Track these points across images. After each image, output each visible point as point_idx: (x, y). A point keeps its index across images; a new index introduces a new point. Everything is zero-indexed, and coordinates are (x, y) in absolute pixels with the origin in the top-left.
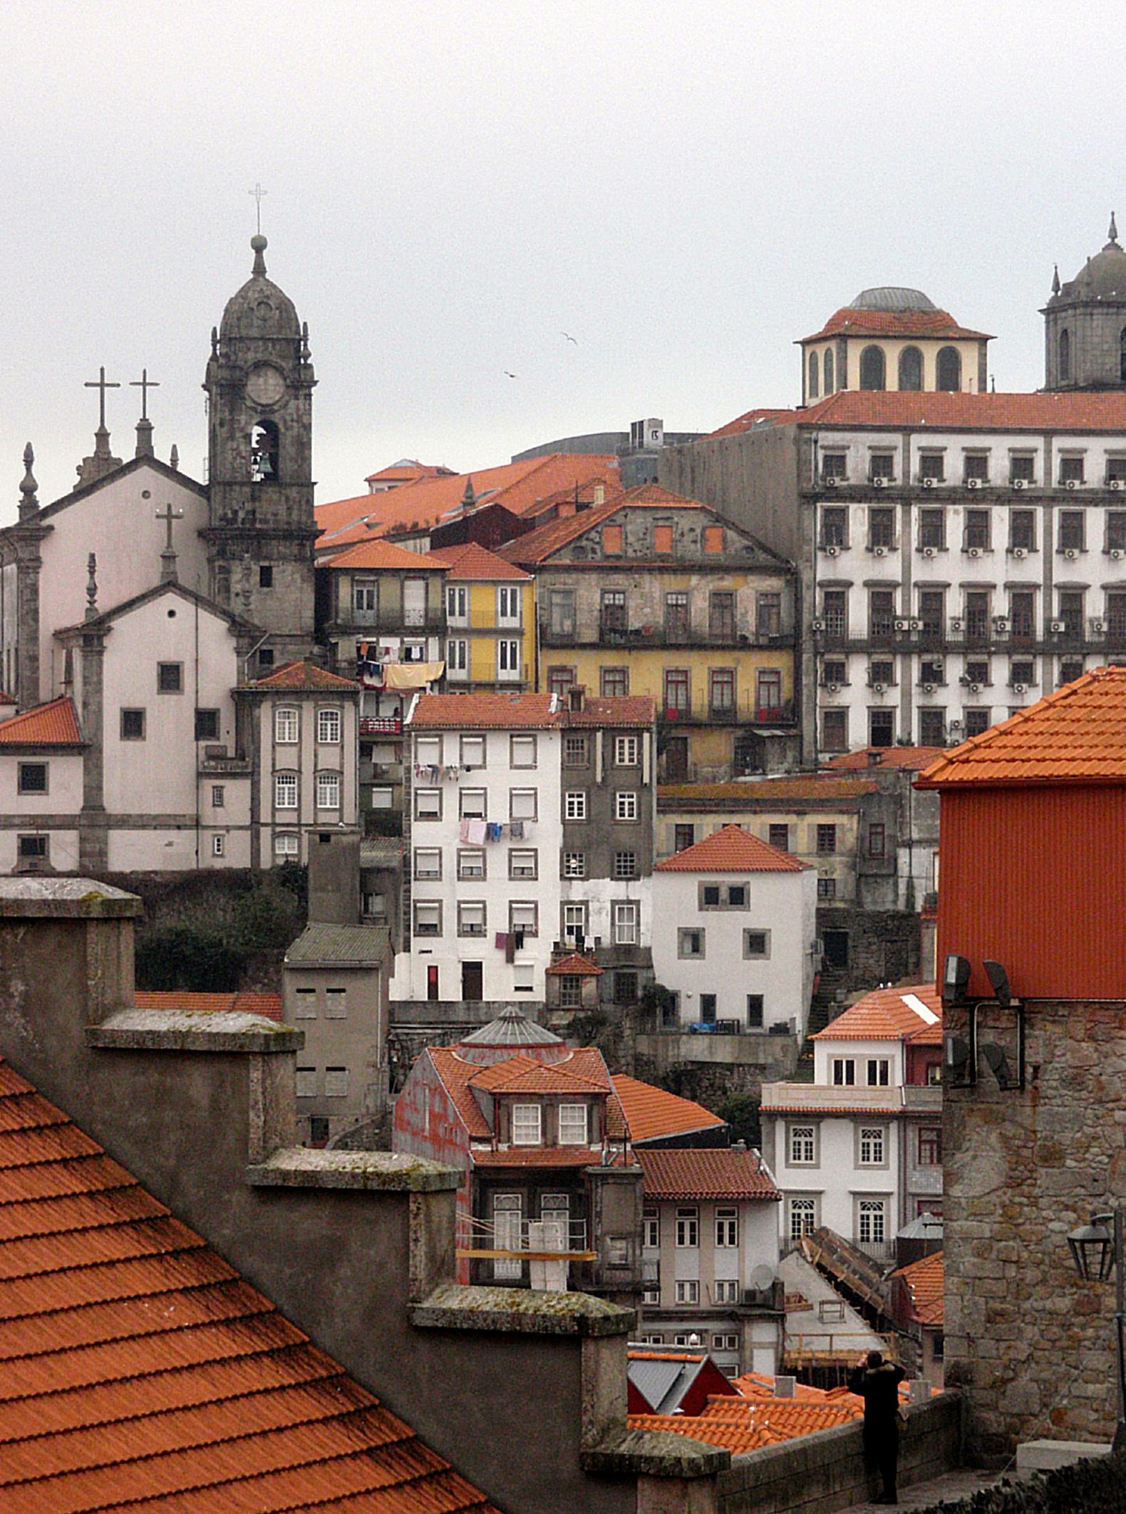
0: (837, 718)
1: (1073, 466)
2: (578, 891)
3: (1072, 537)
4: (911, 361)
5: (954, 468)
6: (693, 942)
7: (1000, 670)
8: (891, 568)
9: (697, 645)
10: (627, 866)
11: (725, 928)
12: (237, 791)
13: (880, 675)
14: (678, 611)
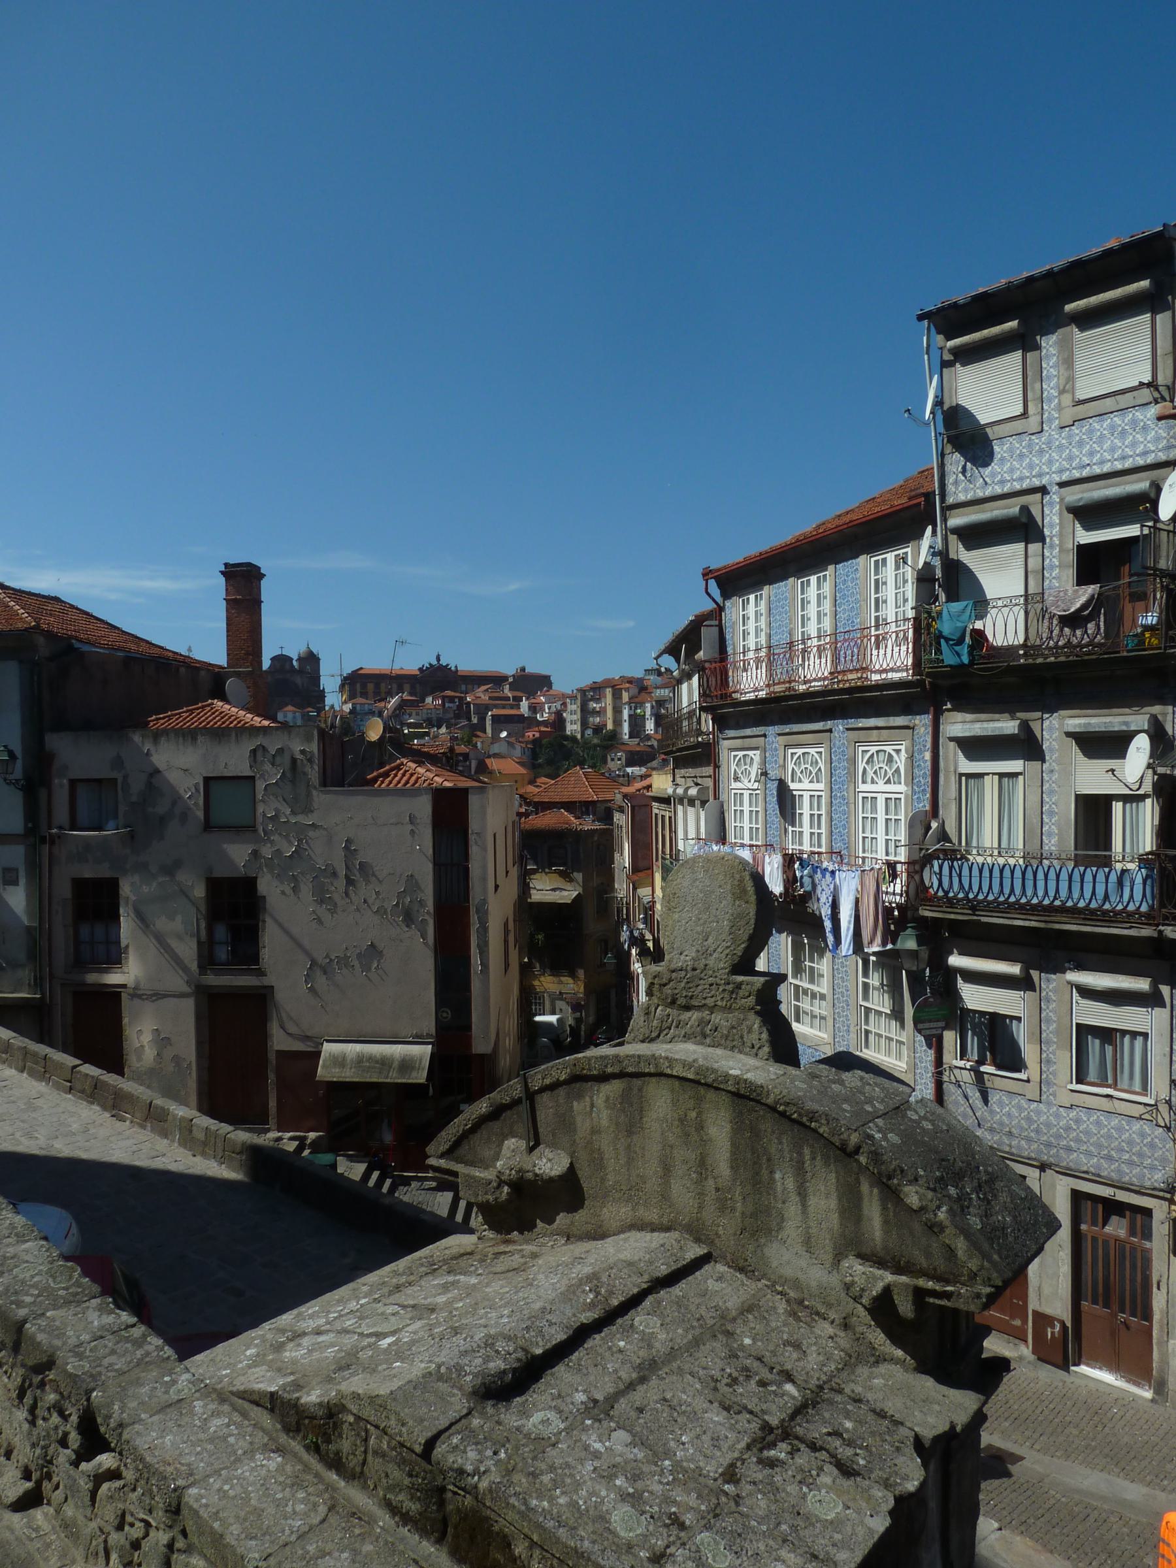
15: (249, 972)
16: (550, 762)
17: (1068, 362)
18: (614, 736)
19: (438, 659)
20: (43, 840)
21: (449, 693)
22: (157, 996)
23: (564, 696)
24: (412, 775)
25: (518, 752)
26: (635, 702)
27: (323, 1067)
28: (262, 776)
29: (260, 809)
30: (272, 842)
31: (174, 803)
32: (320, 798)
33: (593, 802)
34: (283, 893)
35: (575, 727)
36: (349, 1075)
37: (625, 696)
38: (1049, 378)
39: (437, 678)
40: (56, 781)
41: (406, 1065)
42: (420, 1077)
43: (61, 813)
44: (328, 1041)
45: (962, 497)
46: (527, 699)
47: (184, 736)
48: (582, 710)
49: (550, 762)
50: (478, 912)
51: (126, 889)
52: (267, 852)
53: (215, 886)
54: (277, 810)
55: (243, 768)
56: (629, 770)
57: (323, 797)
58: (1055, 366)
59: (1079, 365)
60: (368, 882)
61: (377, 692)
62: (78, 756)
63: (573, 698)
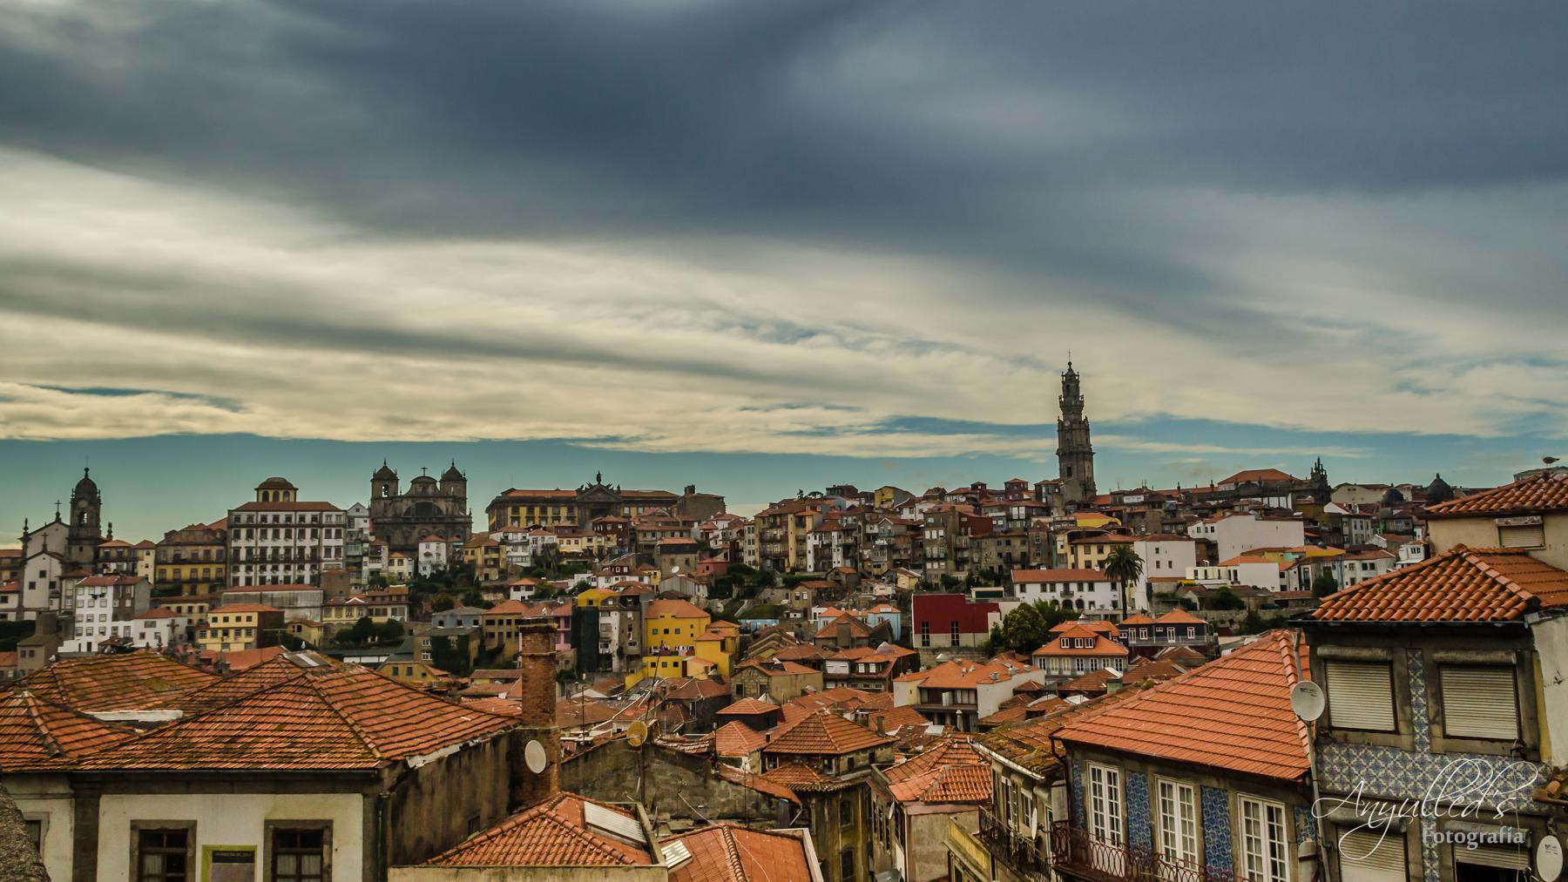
0: (236, 580)
1: (302, 518)
2: (116, 624)
3: (302, 535)
4: (276, 496)
5: (270, 520)
6: (143, 636)
7: (281, 567)
8: (252, 543)
9: (200, 563)
10: (128, 618)
11: (150, 632)
12: (56, 601)
13: (249, 569)
14: (195, 555)
17: (1439, 699)
19: (599, 478)
21: (611, 518)
33: (838, 756)
35: (752, 558)
38: (1419, 706)
39: (598, 504)
45: (1338, 787)
56: (815, 610)
58: (1424, 696)
59: (1448, 705)
61: (529, 518)
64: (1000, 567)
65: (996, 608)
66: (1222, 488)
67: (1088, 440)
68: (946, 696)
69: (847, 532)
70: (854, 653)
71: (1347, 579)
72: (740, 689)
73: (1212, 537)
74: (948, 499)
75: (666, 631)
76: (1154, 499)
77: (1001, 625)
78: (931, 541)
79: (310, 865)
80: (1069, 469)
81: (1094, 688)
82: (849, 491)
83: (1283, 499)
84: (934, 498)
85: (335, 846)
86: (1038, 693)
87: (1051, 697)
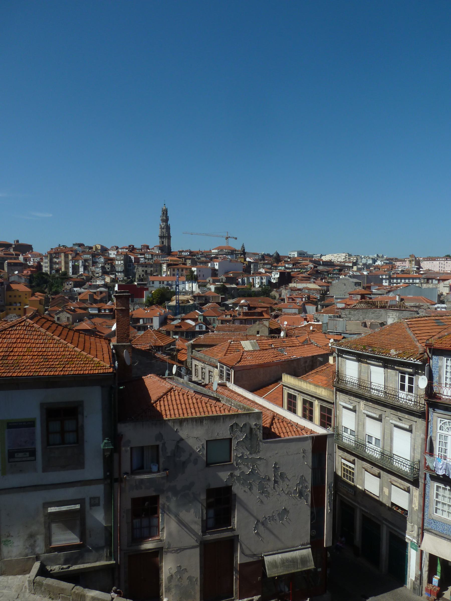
15: (228, 530)
16: (38, 285)
18: (65, 274)
20: (116, 480)
22: (180, 550)
23: (40, 255)
24: (282, 422)
25: (23, 280)
26: (75, 259)
27: (268, 570)
28: (236, 438)
29: (234, 454)
30: (240, 469)
31: (191, 455)
32: (263, 446)
33: (162, 346)
34: (245, 491)
35: (47, 269)
36: (282, 572)
37: (70, 257)
40: (123, 449)
41: (304, 560)
42: (311, 566)
43: (126, 466)
44: (266, 556)
46: (22, 254)
47: (196, 421)
48: (50, 262)
49: (38, 285)
50: (329, 488)
51: (162, 500)
52: (237, 473)
53: (210, 492)
54: (243, 453)
55: (227, 435)
56: (75, 289)
57: (264, 445)
60: (283, 481)
62: (136, 435)
63: (46, 257)
64: (143, 275)
65: (147, 289)
66: (213, 251)
67: (169, 232)
68: (141, 322)
69: (86, 261)
70: (100, 305)
71: (257, 282)
72: (58, 319)
73: (217, 267)
74: (120, 250)
75: (15, 296)
76: (192, 254)
77: (150, 295)
78: (118, 265)
79: (69, 425)
80: (163, 242)
81: (193, 317)
82: (80, 245)
83: (232, 256)
84: (115, 250)
85: (85, 414)
86: (173, 320)
87: (180, 321)
